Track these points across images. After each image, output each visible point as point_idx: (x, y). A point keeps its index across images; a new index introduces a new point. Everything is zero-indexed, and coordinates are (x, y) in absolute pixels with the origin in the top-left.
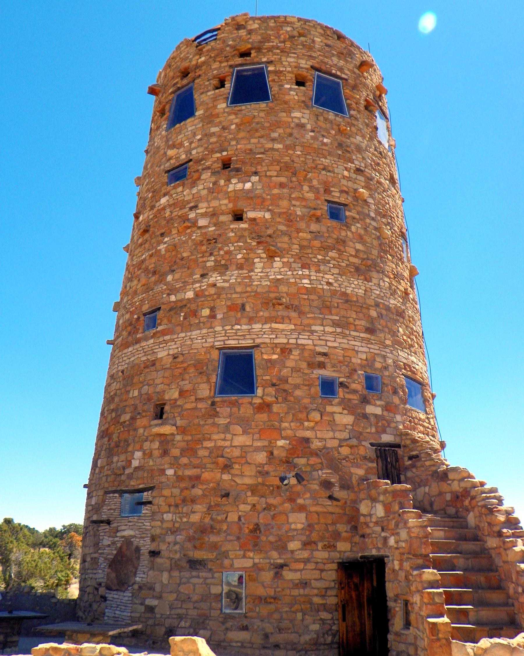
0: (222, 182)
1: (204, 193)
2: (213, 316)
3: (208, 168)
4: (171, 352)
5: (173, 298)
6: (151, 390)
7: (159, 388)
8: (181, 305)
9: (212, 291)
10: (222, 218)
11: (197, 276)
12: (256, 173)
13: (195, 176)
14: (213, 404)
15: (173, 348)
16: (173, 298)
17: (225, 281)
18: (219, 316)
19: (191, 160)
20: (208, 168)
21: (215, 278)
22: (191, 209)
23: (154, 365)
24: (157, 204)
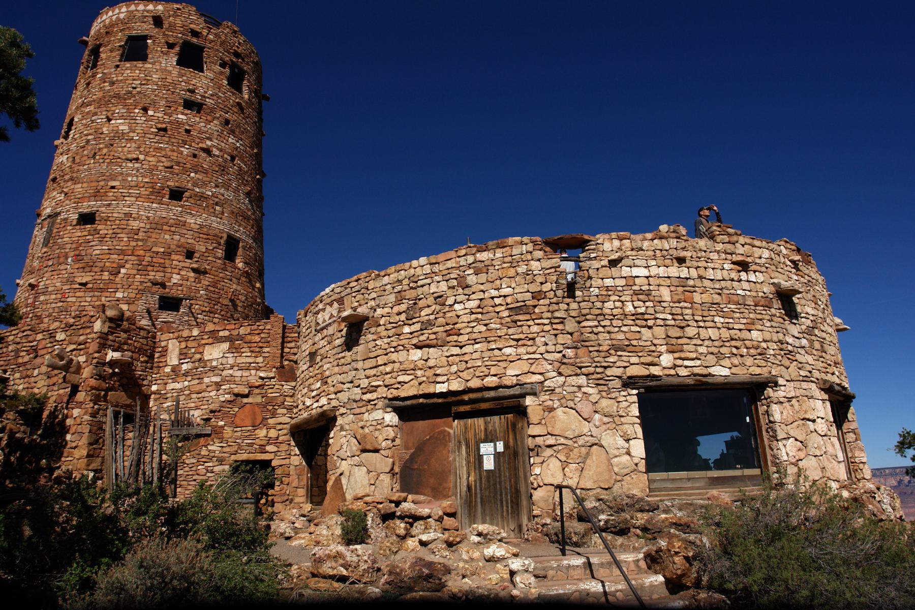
0: (225, 133)
1: (216, 133)
2: (223, 213)
3: (218, 118)
4: (198, 223)
5: (197, 190)
6: (183, 240)
7: (190, 241)
8: (202, 197)
9: (222, 198)
10: (226, 156)
11: (213, 185)
12: (241, 140)
13: (209, 118)
14: (225, 264)
15: (199, 221)
16: (197, 190)
17: (228, 195)
18: (226, 215)
19: (206, 105)
20: (218, 118)
21: (222, 191)
22: (208, 139)
23: (185, 225)
24: (175, 116)
